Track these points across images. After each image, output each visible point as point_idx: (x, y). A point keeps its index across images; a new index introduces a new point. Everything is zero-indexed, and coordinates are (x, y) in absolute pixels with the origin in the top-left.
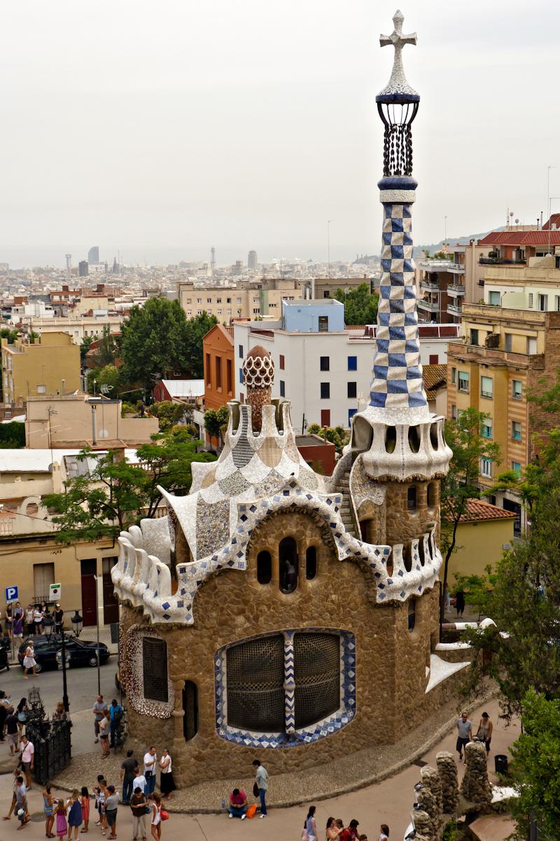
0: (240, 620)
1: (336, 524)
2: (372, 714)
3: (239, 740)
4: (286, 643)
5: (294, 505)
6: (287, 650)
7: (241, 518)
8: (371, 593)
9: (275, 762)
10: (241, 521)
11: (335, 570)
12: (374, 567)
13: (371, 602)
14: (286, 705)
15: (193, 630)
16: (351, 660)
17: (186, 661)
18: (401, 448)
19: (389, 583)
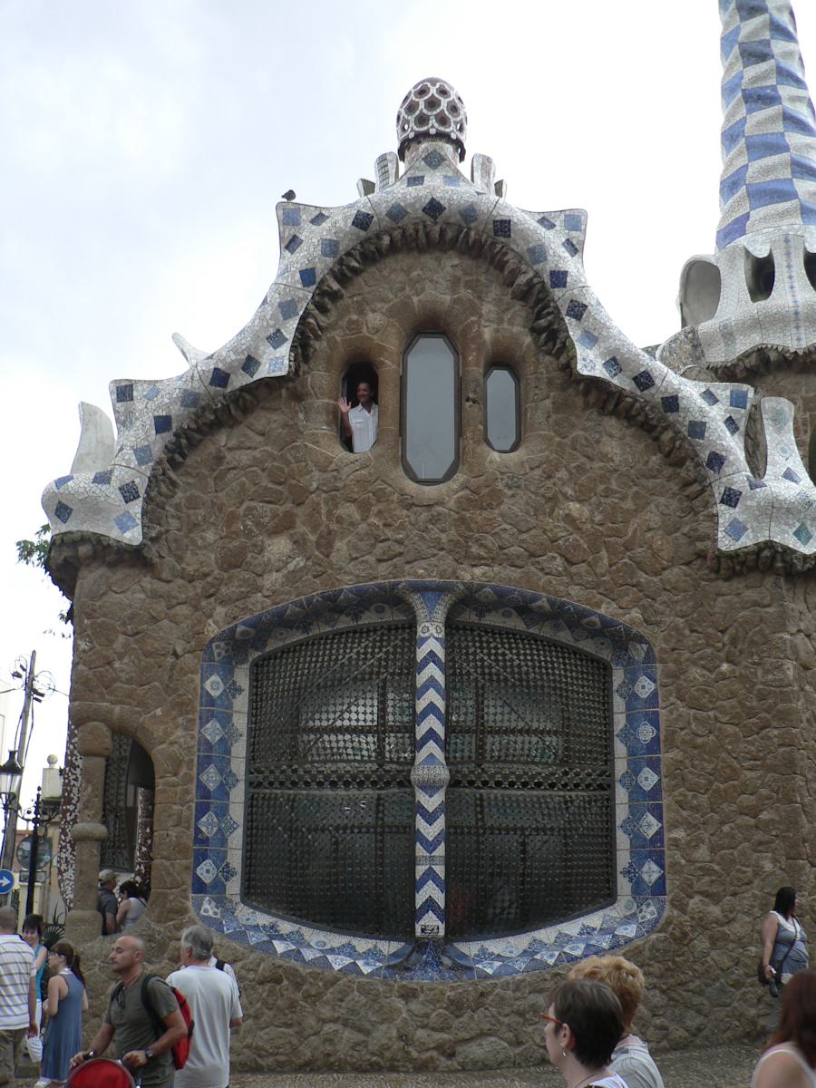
0: (279, 546)
1: (565, 273)
2: (726, 929)
3: (254, 938)
4: (420, 634)
5: (434, 208)
6: (421, 653)
7: (287, 247)
8: (704, 527)
9: (368, 1026)
10: (287, 253)
11: (578, 433)
12: (702, 436)
13: (701, 555)
14: (416, 836)
15: (147, 582)
16: (646, 733)
17: (117, 664)
18: (788, 285)
19: (752, 487)
